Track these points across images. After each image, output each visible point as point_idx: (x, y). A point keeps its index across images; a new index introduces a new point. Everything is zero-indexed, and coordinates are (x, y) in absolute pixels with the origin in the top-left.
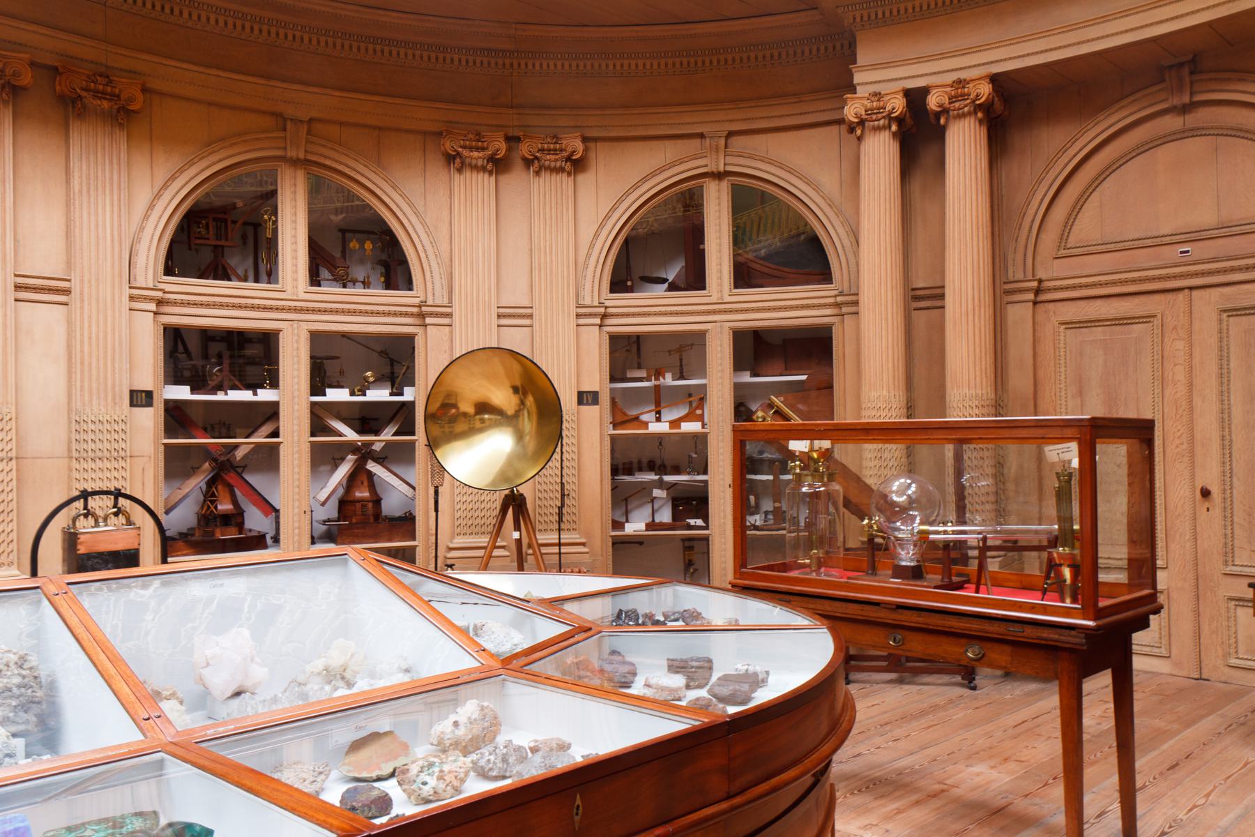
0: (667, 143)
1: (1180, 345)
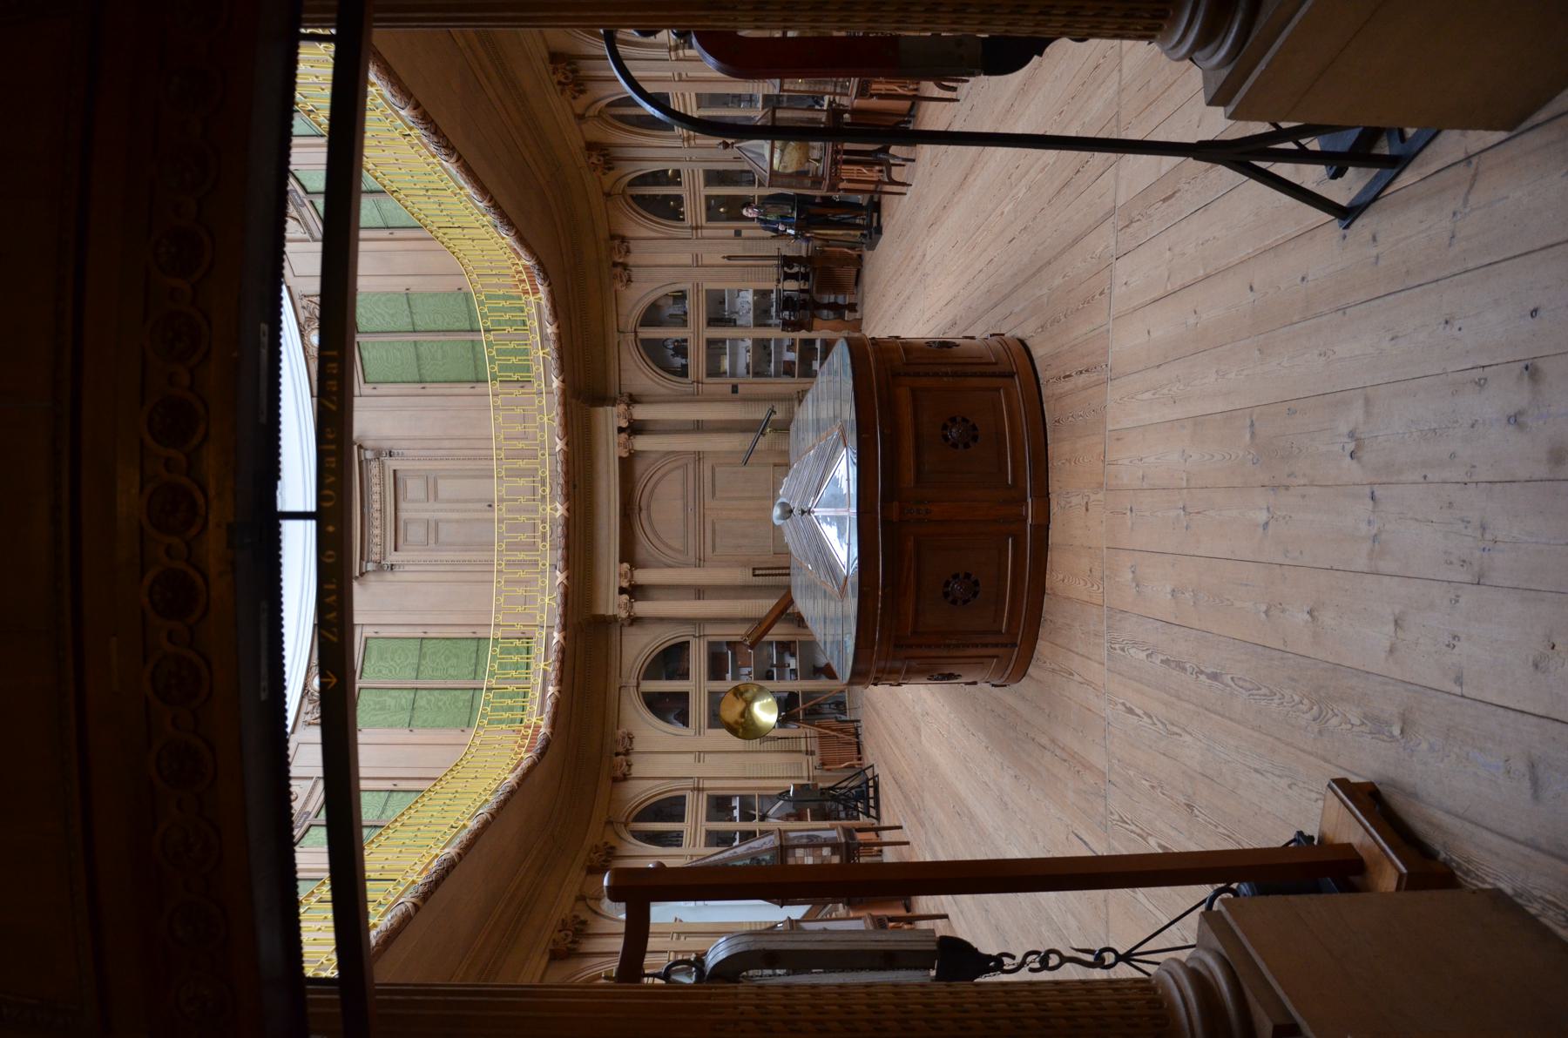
0: (622, 703)
1: (724, 513)
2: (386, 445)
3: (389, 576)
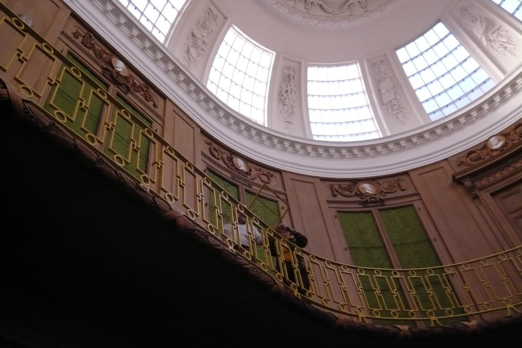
3: (467, 200)
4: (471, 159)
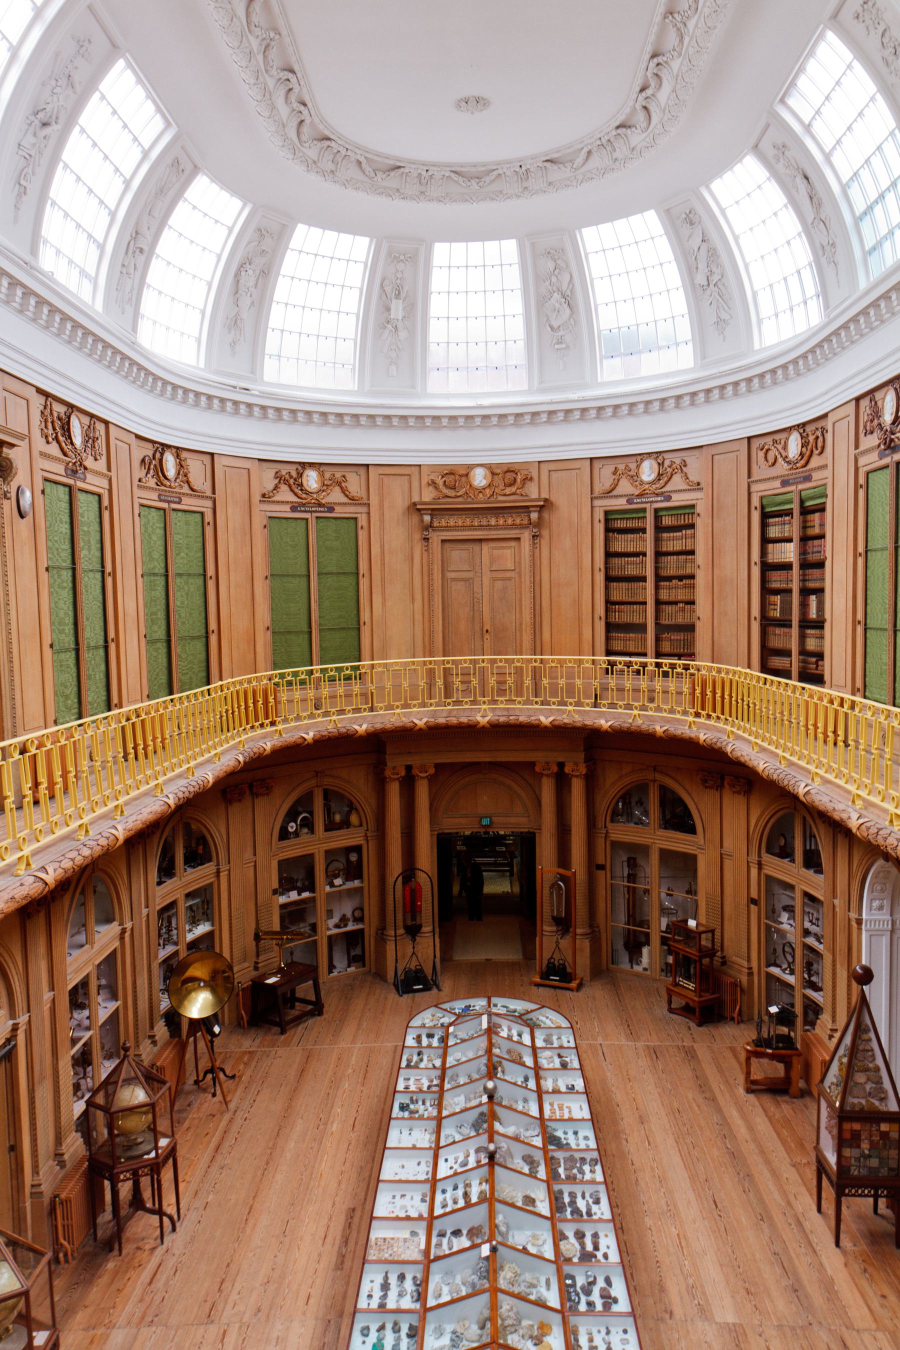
2: (545, 533)
3: (417, 536)
4: (445, 482)
